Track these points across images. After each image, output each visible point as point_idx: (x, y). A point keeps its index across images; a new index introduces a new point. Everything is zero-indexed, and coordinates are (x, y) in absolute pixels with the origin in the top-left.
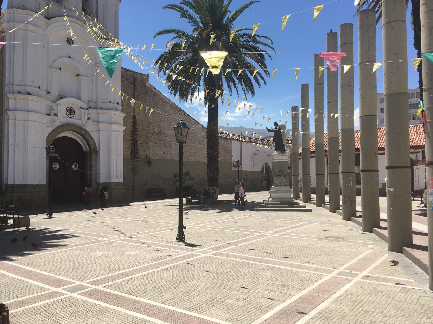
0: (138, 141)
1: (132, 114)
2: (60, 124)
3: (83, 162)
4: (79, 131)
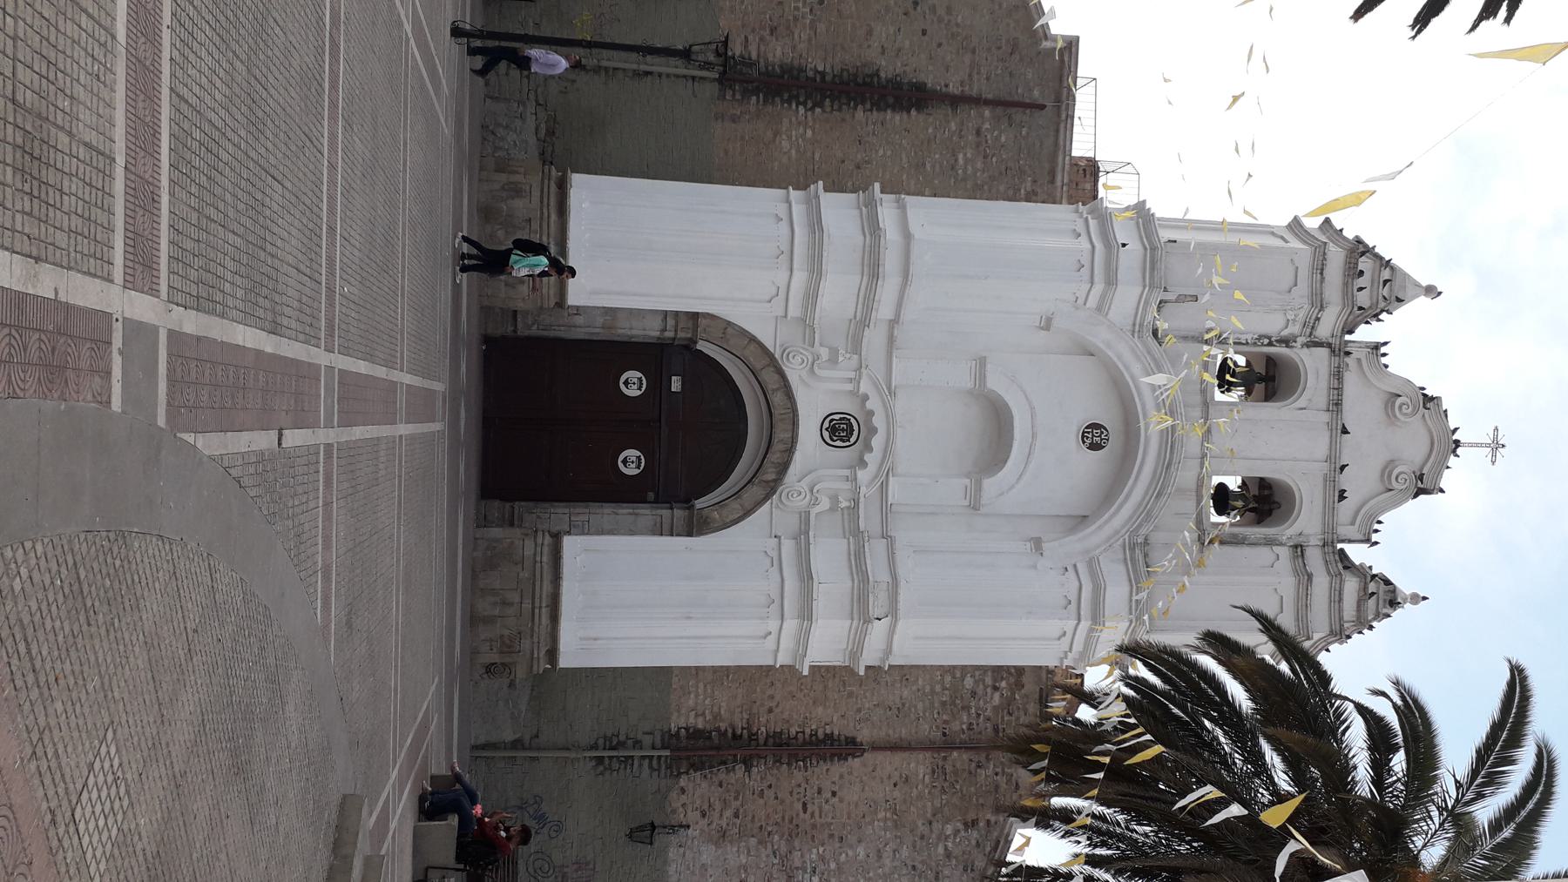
0: (748, 770)
1: (864, 735)
2: (793, 376)
3: (651, 496)
4: (774, 457)
